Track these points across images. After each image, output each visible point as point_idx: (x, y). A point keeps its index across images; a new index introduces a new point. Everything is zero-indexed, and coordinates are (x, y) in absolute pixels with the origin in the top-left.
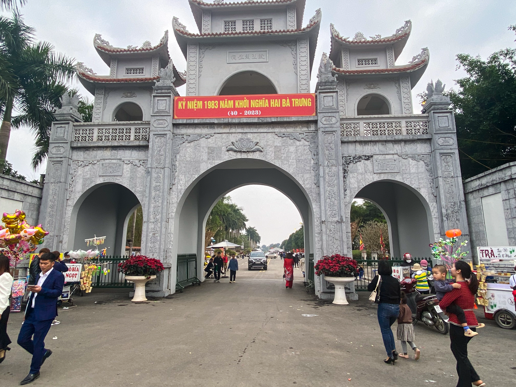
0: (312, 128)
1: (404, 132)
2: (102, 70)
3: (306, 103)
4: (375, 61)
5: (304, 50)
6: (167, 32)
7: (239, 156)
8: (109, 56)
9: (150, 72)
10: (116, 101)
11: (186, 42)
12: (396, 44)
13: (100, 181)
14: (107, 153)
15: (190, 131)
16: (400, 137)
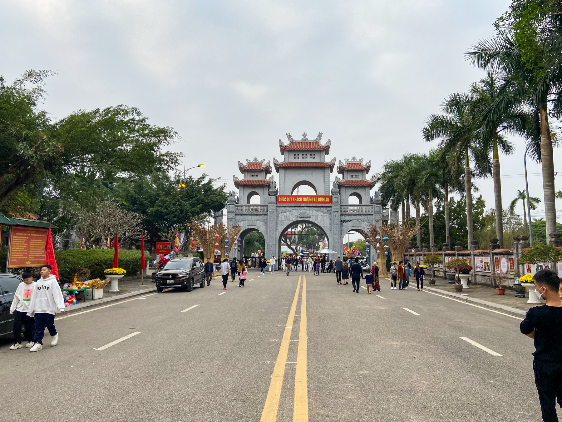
0: (330, 209)
1: (364, 211)
2: (241, 177)
3: (328, 200)
4: (358, 176)
5: (328, 171)
6: (270, 162)
7: (302, 219)
8: (243, 170)
9: (260, 178)
10: (248, 191)
11: (278, 168)
12: (367, 170)
13: (247, 227)
14: (250, 217)
15: (283, 209)
16: (362, 213)
